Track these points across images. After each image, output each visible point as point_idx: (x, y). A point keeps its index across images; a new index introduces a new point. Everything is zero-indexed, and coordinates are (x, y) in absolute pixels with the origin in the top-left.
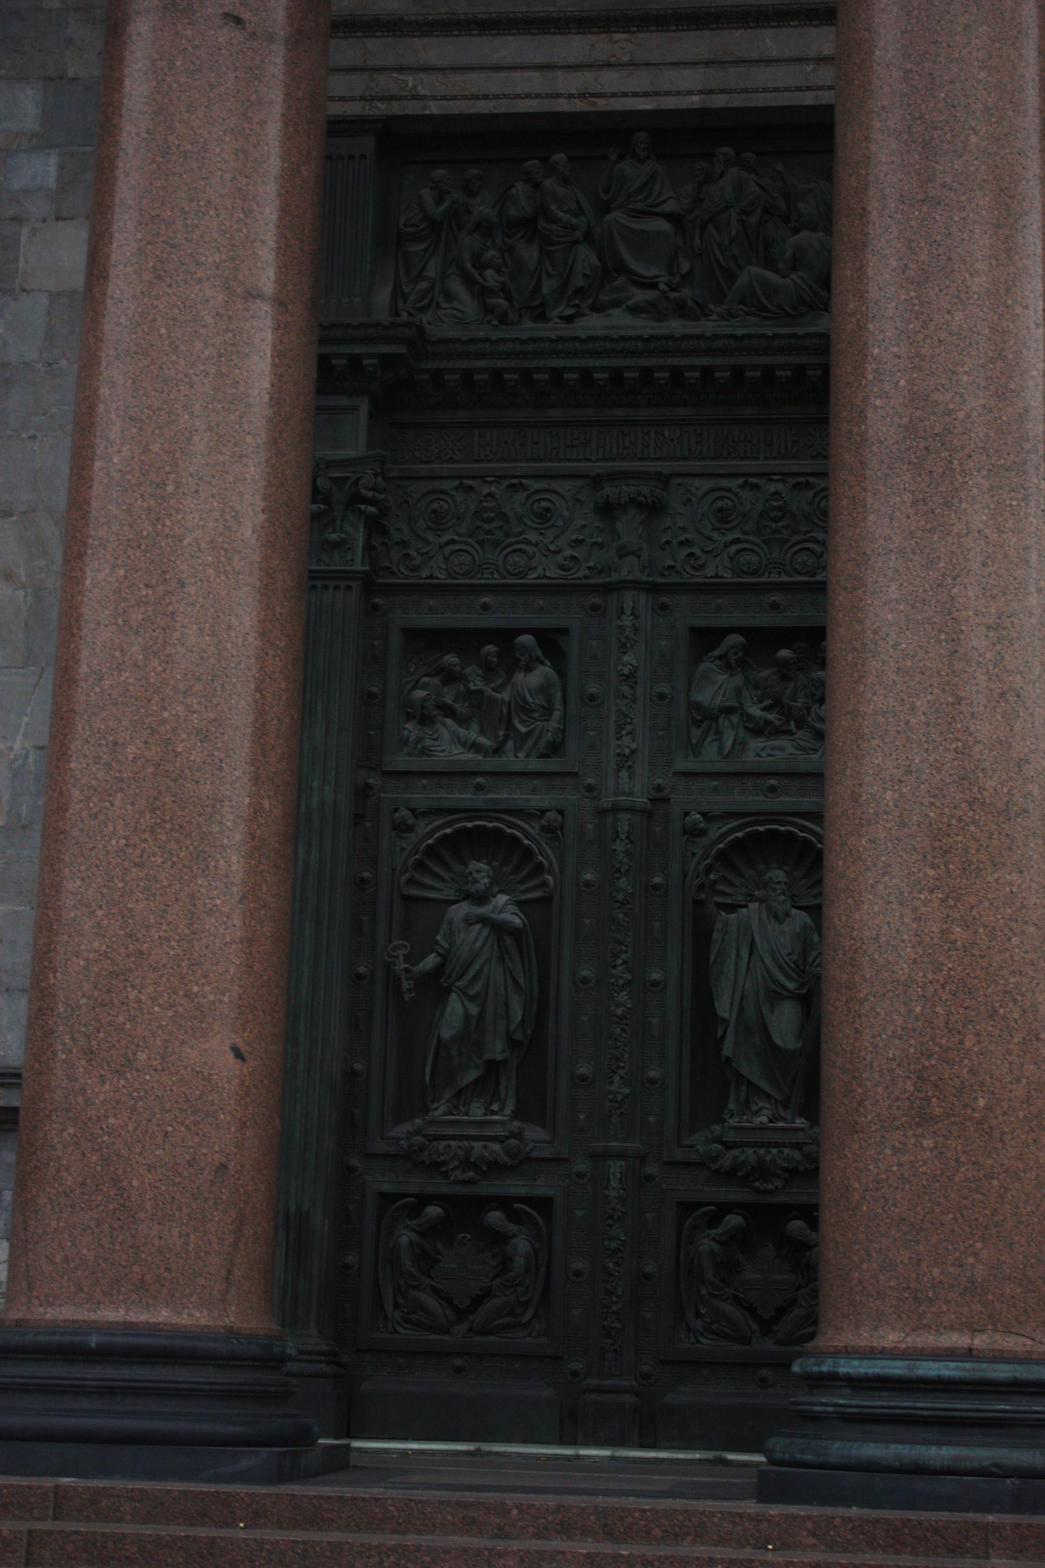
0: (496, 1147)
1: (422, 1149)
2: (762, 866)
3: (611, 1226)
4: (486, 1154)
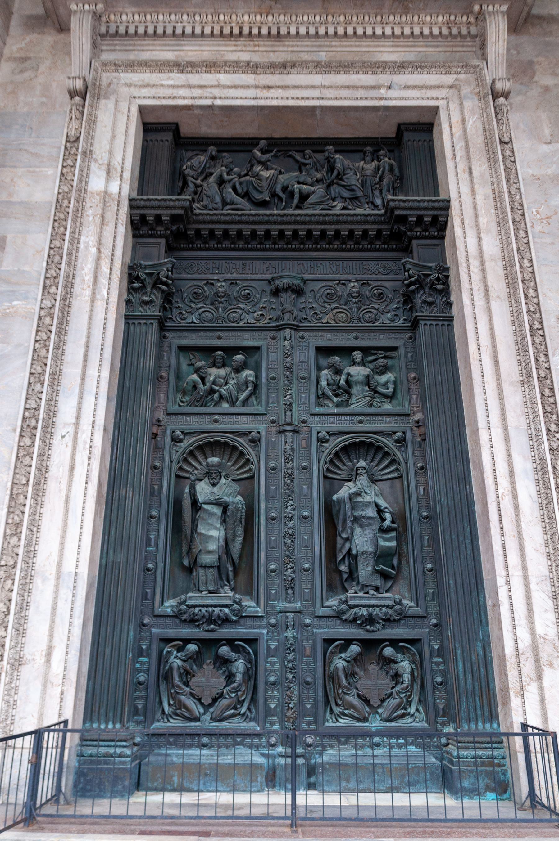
0: (226, 610)
1: (185, 613)
2: (355, 461)
3: (289, 654)
4: (221, 614)
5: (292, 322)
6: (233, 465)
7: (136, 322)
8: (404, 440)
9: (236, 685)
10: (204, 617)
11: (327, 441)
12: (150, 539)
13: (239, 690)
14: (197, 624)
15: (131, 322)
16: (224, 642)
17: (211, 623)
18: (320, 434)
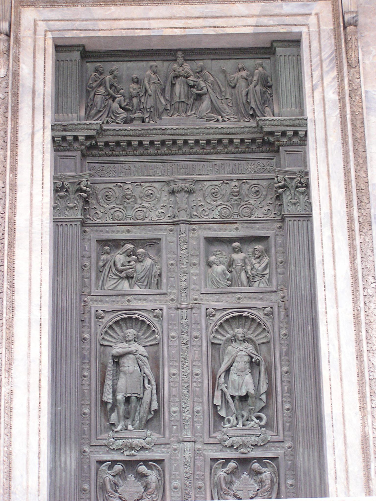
0: (142, 441)
4: (138, 444)
5: (186, 219)
6: (143, 335)
7: (64, 224)
8: (272, 314)
9: (151, 490)
10: (126, 446)
11: (213, 316)
12: (84, 393)
13: (153, 494)
15: (60, 224)
16: (142, 463)
17: (132, 450)
18: (208, 310)
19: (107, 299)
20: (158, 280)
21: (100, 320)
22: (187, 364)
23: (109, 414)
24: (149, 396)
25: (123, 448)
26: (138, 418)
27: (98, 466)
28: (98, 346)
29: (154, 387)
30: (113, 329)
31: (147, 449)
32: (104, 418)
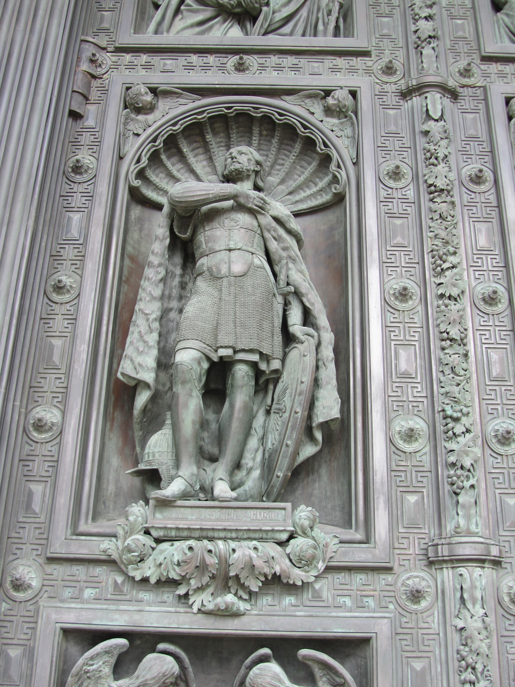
6: (282, 182)
10: (202, 567)
14: (182, 591)
16: (266, 651)
17: (226, 588)
19: (168, 62)
20: (338, 19)
21: (141, 117)
22: (453, 259)
23: (138, 434)
24: (310, 361)
25: (184, 579)
26: (259, 458)
27: (73, 649)
28: (123, 195)
29: (328, 337)
30: (183, 158)
31: (292, 588)
32: (121, 453)
